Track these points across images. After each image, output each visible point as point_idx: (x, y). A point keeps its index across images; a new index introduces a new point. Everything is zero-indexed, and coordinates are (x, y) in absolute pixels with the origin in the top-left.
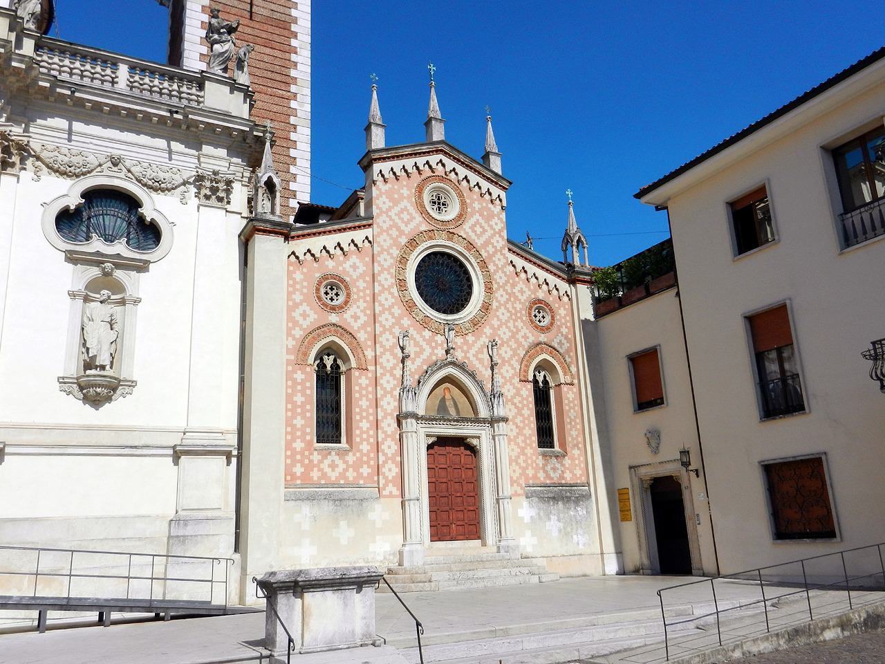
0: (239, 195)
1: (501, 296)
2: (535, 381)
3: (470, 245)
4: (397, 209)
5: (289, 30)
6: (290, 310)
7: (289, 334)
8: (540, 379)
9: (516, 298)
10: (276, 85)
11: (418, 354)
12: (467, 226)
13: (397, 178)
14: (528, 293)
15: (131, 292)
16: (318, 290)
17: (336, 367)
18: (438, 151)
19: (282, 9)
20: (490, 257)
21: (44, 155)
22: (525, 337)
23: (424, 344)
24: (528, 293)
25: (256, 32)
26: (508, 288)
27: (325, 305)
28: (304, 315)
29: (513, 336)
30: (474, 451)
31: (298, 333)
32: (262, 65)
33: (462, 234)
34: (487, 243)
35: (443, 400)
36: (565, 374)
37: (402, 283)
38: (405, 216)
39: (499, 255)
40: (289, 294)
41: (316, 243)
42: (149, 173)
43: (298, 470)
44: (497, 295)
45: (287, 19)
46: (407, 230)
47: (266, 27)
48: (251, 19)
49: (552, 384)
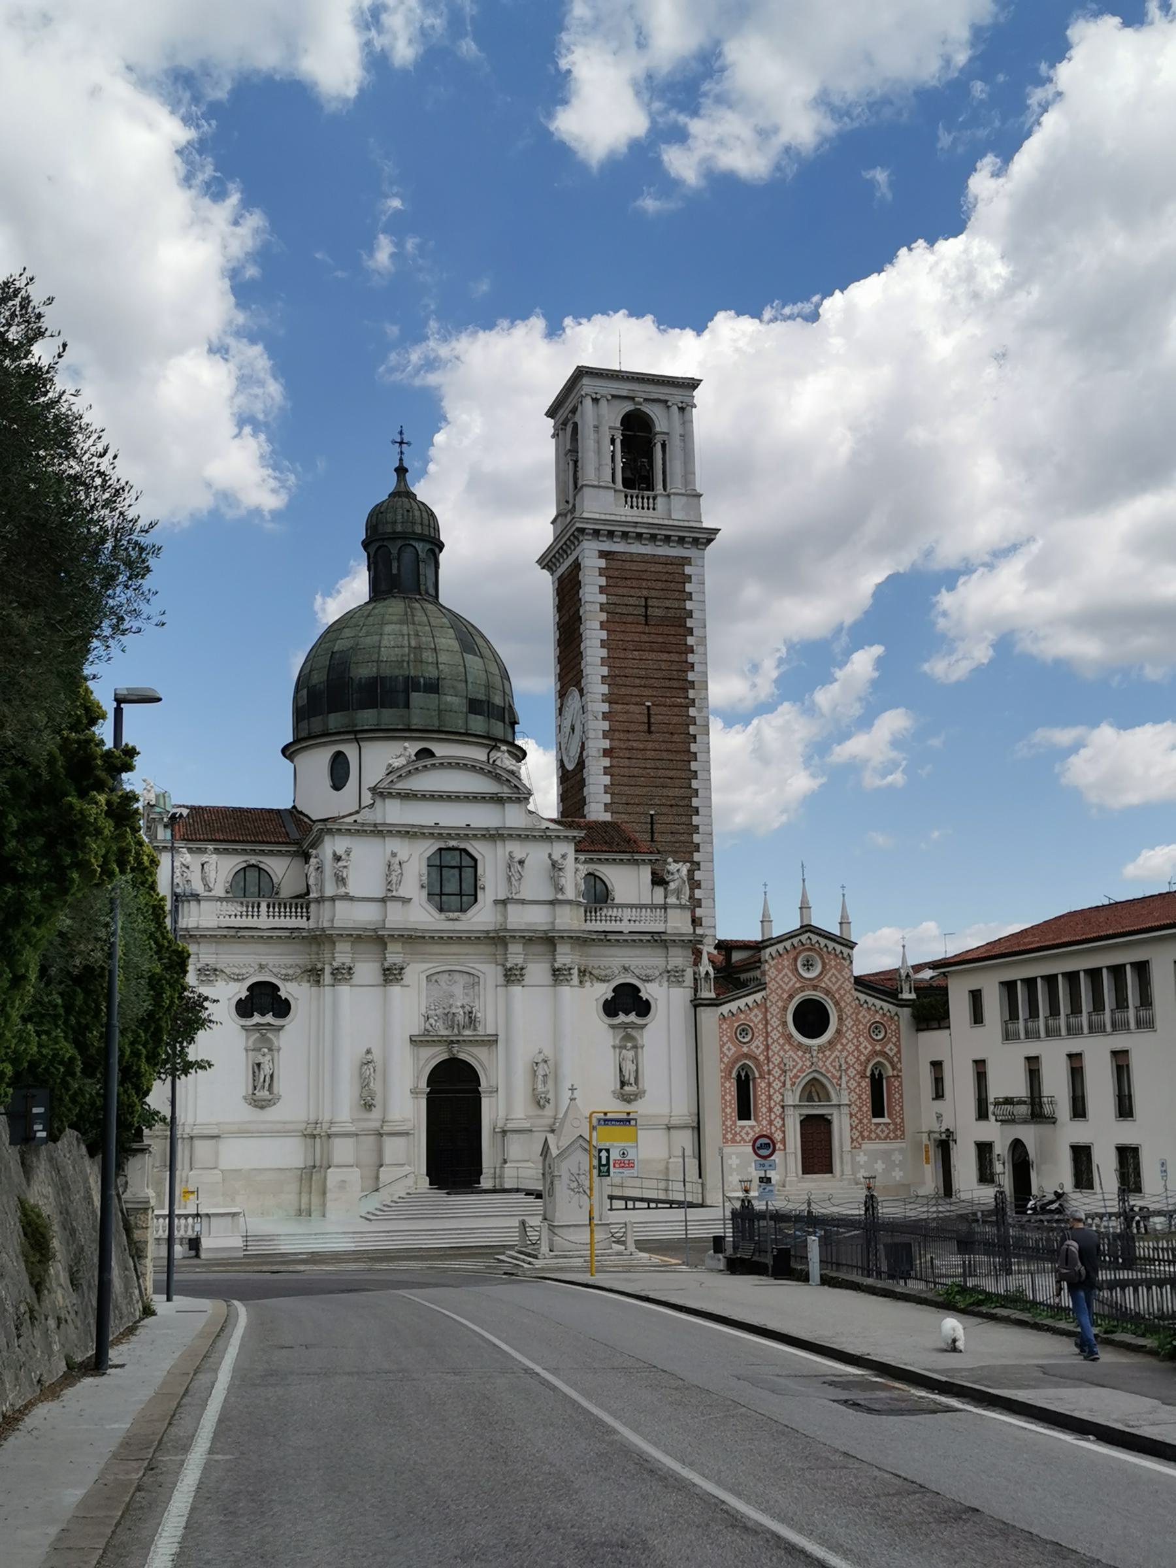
0: (689, 973)
1: (849, 1023)
2: (873, 1074)
3: (827, 992)
4: (781, 976)
5: (685, 626)
6: (722, 1046)
7: (722, 1061)
8: (877, 1073)
9: (860, 1022)
10: (674, 693)
11: (794, 1067)
12: (825, 979)
13: (780, 955)
14: (868, 1017)
15: (640, 1042)
16: (736, 1033)
17: (747, 1076)
18: (806, 932)
19: (676, 604)
20: (842, 997)
21: (593, 972)
22: (866, 1048)
23: (798, 1060)
24: (868, 1017)
25: (653, 638)
26: (854, 1016)
27: (740, 1042)
28: (729, 1049)
29: (857, 1047)
30: (829, 1123)
31: (726, 1060)
32: (660, 675)
33: (823, 985)
34: (839, 989)
35: (810, 1092)
36: (893, 1069)
37: (785, 1024)
38: (786, 979)
39: (848, 995)
40: (721, 1037)
41: (733, 1006)
42: (644, 973)
43: (729, 1136)
44: (846, 1023)
45: (679, 613)
46: (787, 988)
47: (661, 630)
48: (647, 624)
49: (884, 1076)
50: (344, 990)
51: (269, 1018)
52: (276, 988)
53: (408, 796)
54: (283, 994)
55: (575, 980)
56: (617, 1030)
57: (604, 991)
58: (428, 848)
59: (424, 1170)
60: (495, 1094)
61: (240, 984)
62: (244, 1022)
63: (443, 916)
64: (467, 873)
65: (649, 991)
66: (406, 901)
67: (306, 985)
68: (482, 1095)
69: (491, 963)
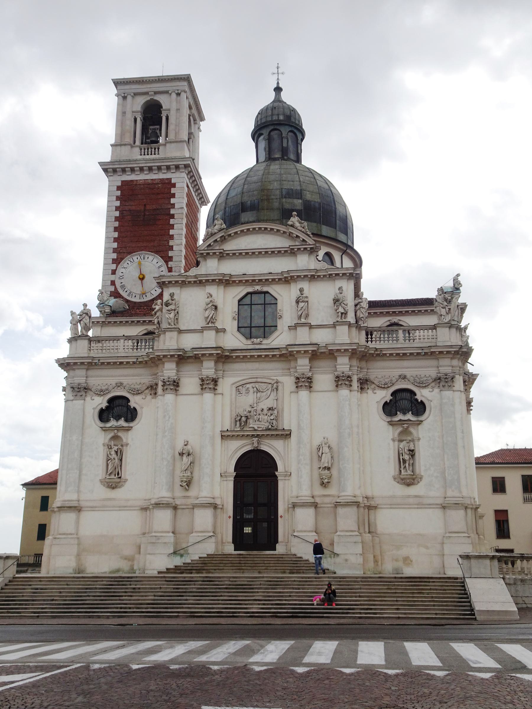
50: (170, 397)
51: (122, 422)
52: (128, 400)
53: (223, 256)
54: (132, 404)
55: (355, 384)
56: (395, 427)
57: (385, 395)
58: (240, 291)
59: (230, 538)
60: (290, 478)
61: (102, 397)
62: (102, 425)
63: (249, 342)
64: (269, 309)
65: (422, 394)
66: (218, 331)
67: (149, 397)
68: (279, 478)
69: (286, 375)
